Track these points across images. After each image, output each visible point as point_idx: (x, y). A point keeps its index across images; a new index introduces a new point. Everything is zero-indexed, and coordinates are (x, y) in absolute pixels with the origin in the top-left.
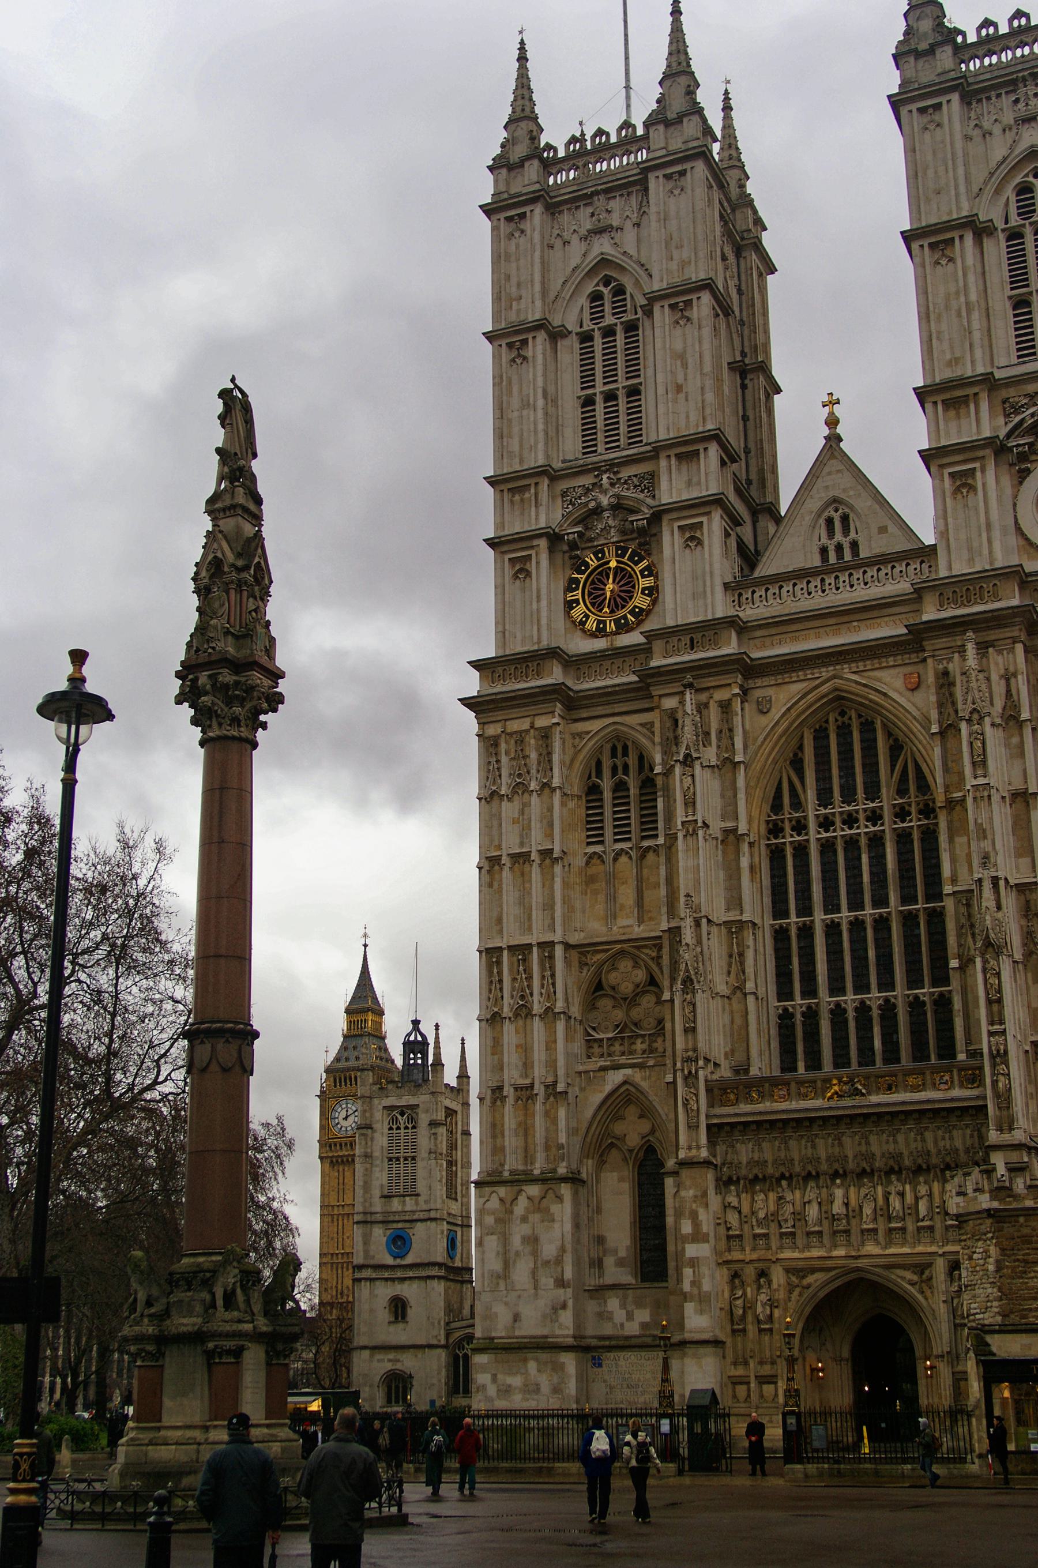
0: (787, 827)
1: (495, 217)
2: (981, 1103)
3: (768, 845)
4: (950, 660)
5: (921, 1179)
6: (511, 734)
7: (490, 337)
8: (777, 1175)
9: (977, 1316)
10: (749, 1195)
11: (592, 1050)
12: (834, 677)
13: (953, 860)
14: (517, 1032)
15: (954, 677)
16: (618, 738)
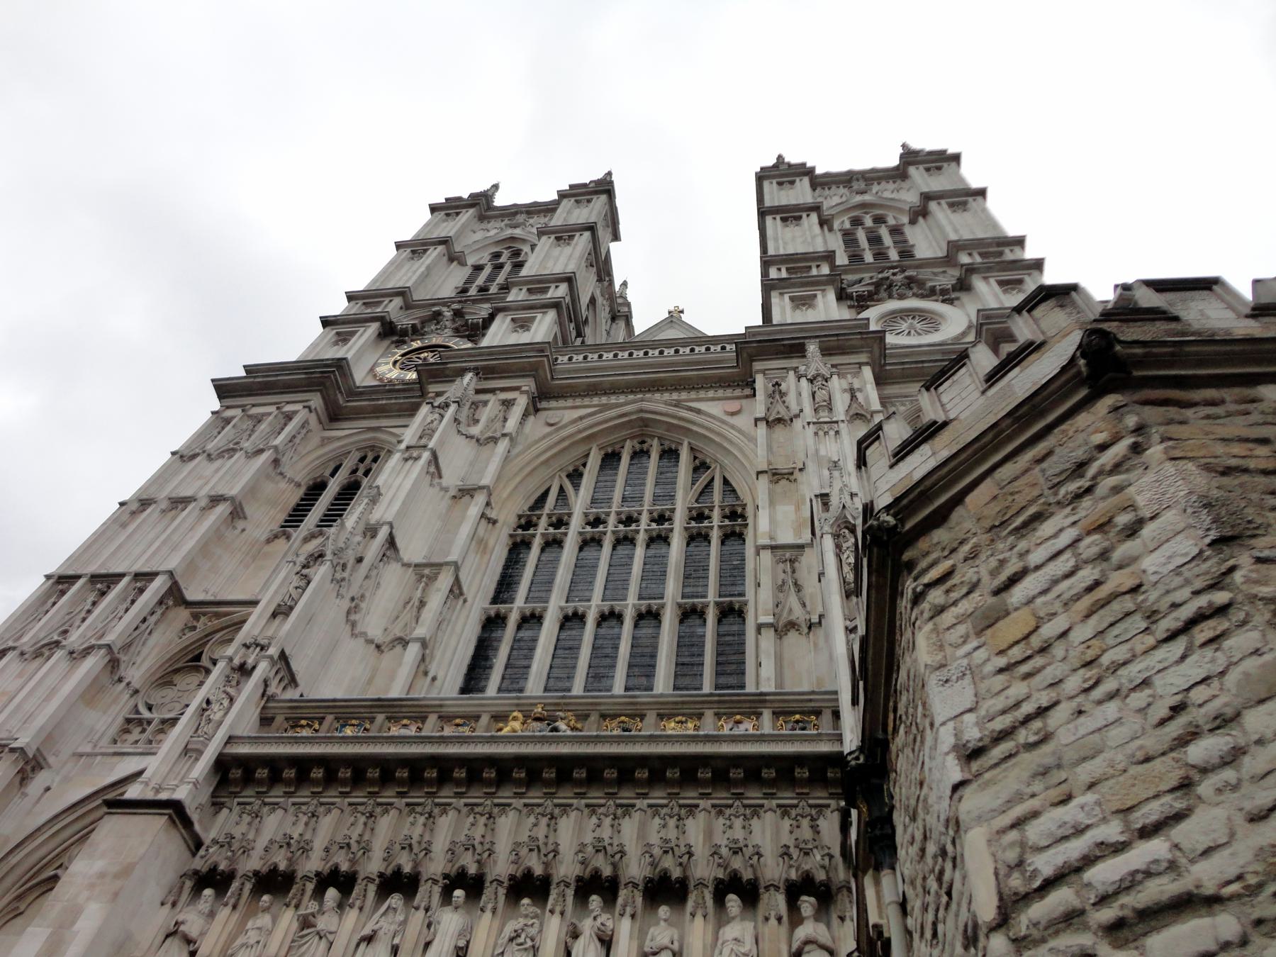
0: (543, 522)
1: (436, 214)
2: (825, 748)
3: (511, 536)
4: (784, 378)
5: (664, 911)
6: (250, 417)
7: (399, 246)
8: (325, 868)
9: (1105, 873)
10: (236, 916)
11: (126, 736)
12: (642, 400)
13: (772, 521)
14: (20, 675)
15: (789, 388)
16: (372, 448)
